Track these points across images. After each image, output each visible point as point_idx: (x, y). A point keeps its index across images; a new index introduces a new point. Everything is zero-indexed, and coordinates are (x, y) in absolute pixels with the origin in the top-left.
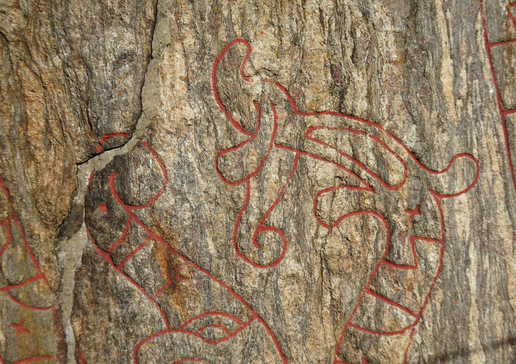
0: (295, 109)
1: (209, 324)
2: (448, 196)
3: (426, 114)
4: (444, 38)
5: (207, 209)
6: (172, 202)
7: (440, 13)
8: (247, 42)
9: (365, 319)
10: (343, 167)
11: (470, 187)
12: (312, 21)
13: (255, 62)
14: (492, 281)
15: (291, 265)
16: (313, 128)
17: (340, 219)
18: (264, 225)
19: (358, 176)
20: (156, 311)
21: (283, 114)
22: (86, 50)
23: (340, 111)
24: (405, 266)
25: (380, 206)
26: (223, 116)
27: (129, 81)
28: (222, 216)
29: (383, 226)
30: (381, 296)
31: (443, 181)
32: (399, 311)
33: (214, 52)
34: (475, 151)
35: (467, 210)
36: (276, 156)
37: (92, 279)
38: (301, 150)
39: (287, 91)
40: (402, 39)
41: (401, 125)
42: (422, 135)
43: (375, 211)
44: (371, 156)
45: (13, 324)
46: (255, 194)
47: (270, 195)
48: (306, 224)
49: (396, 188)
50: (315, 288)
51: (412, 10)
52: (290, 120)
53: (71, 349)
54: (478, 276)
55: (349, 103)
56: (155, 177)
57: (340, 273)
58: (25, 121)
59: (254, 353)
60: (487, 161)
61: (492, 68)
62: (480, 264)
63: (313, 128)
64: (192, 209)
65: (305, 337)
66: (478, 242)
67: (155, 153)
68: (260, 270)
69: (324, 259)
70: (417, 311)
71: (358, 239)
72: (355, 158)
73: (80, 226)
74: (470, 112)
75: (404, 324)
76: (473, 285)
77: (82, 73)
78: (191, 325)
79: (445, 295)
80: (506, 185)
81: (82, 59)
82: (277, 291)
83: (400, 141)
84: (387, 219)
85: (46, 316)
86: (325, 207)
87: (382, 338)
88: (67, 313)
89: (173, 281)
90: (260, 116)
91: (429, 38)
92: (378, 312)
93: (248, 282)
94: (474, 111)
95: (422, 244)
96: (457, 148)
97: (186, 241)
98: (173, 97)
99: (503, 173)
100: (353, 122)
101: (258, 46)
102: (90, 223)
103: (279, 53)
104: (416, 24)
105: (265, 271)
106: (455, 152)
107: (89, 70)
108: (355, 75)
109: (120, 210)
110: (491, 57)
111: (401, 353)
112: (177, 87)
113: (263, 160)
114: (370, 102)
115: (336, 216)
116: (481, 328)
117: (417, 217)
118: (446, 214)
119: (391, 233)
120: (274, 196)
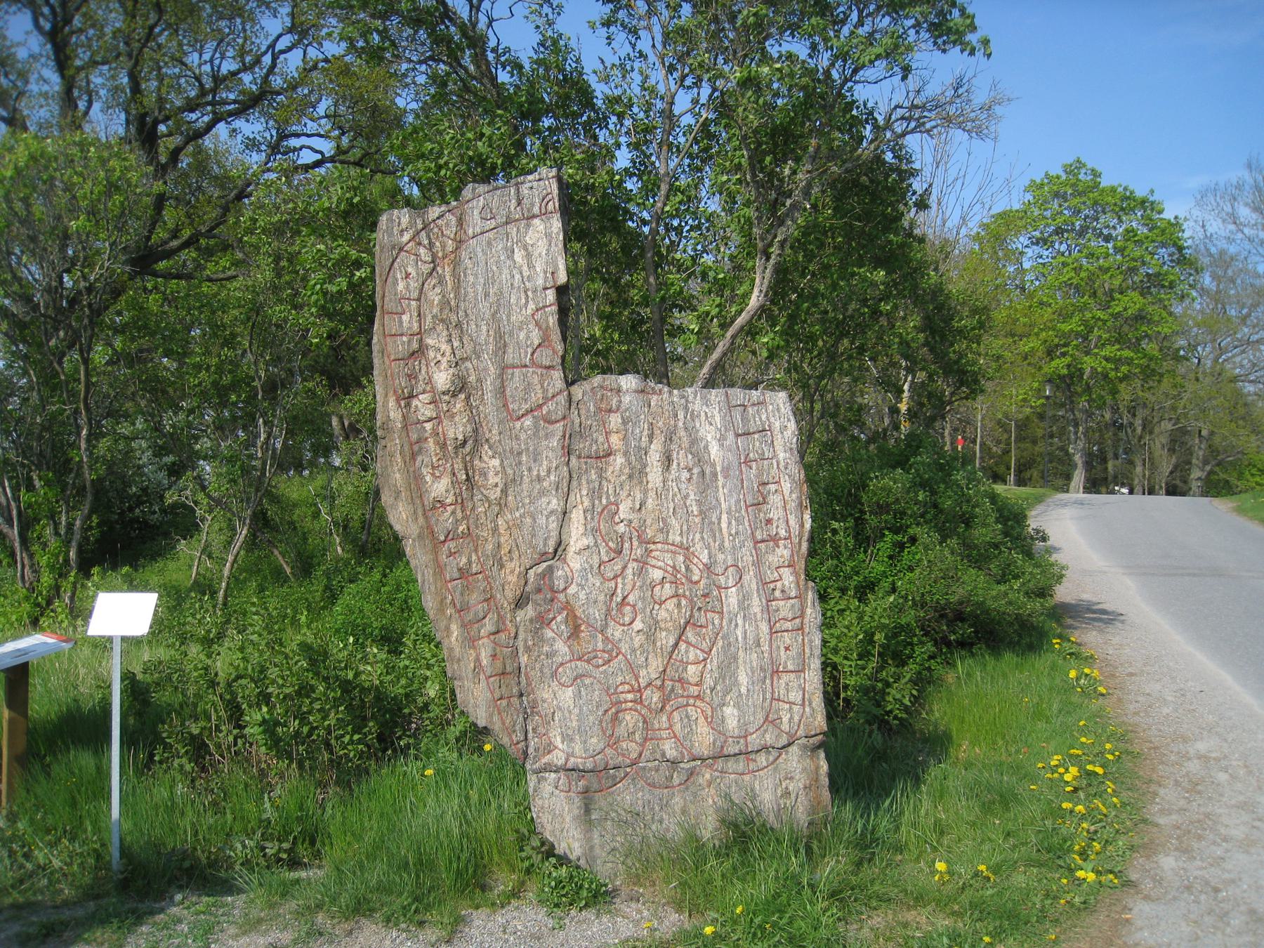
0: (643, 541)
8: (617, 505)
12: (652, 494)
14: (751, 636)
21: (635, 543)
27: (555, 525)
30: (689, 643)
31: (722, 580)
43: (684, 596)
46: (620, 586)
47: (629, 587)
49: (697, 583)
72: (674, 567)
84: (691, 601)
88: (521, 651)
92: (687, 652)
113: (625, 567)
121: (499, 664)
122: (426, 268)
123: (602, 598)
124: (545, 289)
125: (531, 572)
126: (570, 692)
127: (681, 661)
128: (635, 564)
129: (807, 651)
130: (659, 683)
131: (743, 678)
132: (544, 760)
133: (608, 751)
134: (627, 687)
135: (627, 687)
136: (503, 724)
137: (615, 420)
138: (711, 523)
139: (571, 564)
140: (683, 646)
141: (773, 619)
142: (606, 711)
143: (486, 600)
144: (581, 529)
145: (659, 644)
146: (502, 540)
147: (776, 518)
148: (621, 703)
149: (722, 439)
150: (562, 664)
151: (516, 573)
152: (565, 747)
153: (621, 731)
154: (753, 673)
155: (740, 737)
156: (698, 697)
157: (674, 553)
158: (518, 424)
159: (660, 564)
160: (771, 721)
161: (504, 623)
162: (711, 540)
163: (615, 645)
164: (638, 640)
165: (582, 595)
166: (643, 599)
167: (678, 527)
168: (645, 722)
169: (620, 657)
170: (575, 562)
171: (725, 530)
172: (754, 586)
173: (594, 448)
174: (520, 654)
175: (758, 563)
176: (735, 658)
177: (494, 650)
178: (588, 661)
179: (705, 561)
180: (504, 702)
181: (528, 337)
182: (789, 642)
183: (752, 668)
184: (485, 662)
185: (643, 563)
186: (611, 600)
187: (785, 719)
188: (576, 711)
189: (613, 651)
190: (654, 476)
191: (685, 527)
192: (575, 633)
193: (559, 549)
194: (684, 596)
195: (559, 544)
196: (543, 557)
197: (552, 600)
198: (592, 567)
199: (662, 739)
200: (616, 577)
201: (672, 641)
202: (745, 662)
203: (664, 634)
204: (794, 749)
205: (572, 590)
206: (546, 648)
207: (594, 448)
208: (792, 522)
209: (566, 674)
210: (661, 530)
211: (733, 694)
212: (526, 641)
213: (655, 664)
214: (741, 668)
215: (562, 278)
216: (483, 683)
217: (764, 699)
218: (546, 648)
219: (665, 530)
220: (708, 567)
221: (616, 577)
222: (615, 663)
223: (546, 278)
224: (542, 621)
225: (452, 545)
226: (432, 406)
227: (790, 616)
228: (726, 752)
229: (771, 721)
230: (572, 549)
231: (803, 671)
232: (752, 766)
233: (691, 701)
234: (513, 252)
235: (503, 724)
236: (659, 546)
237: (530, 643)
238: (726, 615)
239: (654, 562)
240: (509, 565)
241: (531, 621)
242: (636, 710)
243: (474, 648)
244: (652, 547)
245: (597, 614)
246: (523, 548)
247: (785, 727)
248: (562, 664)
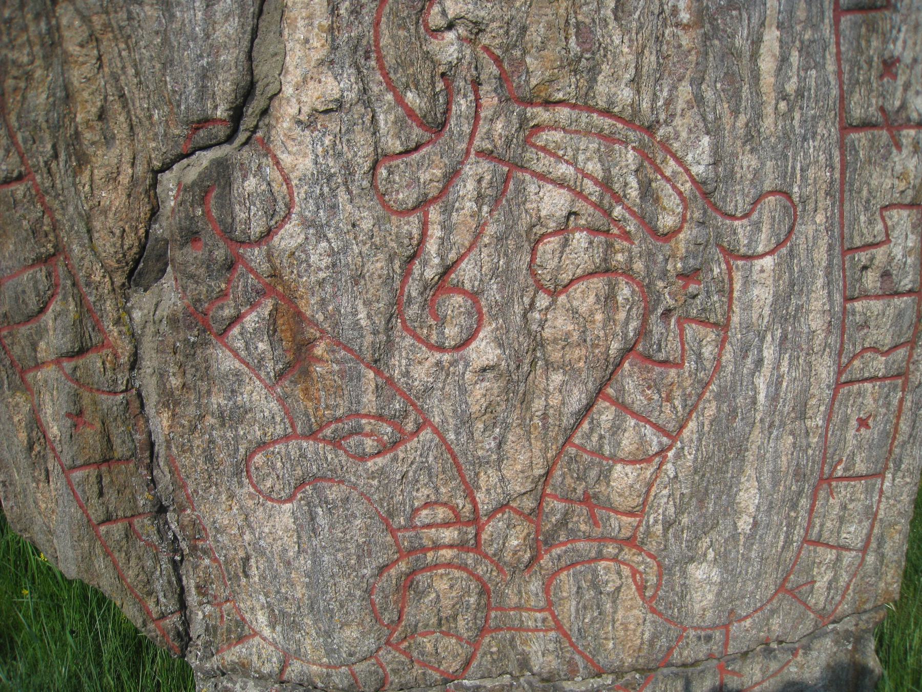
1: (357, 431)
3: (727, 120)
9: (595, 438)
10: (586, 199)
11: (779, 245)
16: (538, 128)
17: (571, 282)
19: (608, 213)
20: (274, 405)
21: (490, 101)
24: (665, 363)
26: (389, 97)
30: (624, 407)
32: (648, 431)
35: (770, 282)
36: (476, 173)
39: (498, 61)
41: (684, 135)
43: (628, 273)
44: (633, 182)
46: (436, 232)
47: (462, 238)
49: (669, 236)
55: (602, 88)
58: (67, 96)
62: (777, 366)
63: (538, 128)
64: (332, 253)
66: (778, 333)
68: (438, 355)
72: (606, 184)
73: (164, 271)
74: (796, 123)
75: (655, 448)
78: (328, 432)
79: (719, 409)
80: (830, 247)
82: (463, 390)
87: (619, 467)
94: (803, 122)
97: (323, 302)
105: (446, 357)
110: (837, 33)
113: (452, 176)
115: (565, 277)
118: (737, 286)
121: (91, 435)
123: (377, 265)
125: (168, 180)
126: (285, 516)
127: (598, 452)
128: (485, 167)
129: (904, 427)
130: (528, 504)
131: (749, 497)
132: (232, 655)
133: (387, 656)
134: (441, 513)
135: (441, 513)
136: (121, 577)
138: (731, 53)
139: (286, 159)
140: (606, 414)
141: (848, 347)
142: (382, 569)
143: (41, 260)
144: (319, 47)
145: (538, 404)
146: (76, 76)
147: (908, 57)
148: (424, 549)
150: (262, 445)
151: (124, 179)
152: (279, 639)
153: (421, 612)
154: (775, 483)
155: (714, 627)
156: (630, 541)
157: (608, 138)
159: (564, 169)
160: (790, 590)
161: (98, 327)
162: (724, 108)
163: (414, 401)
164: (479, 394)
165: (318, 256)
166: (505, 276)
167: (627, 54)
168: (484, 591)
169: (426, 435)
170: (298, 154)
171: (768, 80)
172: (821, 255)
174: (150, 410)
175: (841, 191)
176: (741, 450)
177: (76, 398)
178: (336, 442)
179: (698, 170)
180: (117, 529)
183: (775, 472)
184: (54, 430)
185: (510, 164)
186: (407, 273)
187: (821, 583)
188: (305, 563)
189: (406, 412)
191: (650, 59)
192: (297, 362)
193: (247, 110)
194: (628, 273)
195: (247, 92)
196: (198, 132)
197: (230, 266)
198: (348, 169)
199: (521, 629)
200: (423, 204)
201: (577, 399)
202: (761, 458)
203: (557, 378)
205: (290, 237)
206: (218, 400)
209: (274, 467)
210: (572, 65)
211: (719, 536)
212: (162, 375)
213: (523, 458)
214: (750, 471)
216: (57, 483)
217: (788, 542)
218: (218, 400)
219: (586, 63)
220: (705, 191)
221: (423, 204)
222: (410, 450)
224: (201, 325)
227: (888, 341)
229: (790, 590)
230: (288, 111)
231: (881, 475)
233: (611, 549)
235: (121, 577)
236: (564, 113)
237: (175, 382)
238: (736, 335)
239: (544, 163)
240: (104, 159)
241: (173, 321)
242: (463, 567)
243: (26, 388)
244: (542, 115)
245: (361, 314)
246: (140, 104)
247: (818, 599)
248: (262, 445)
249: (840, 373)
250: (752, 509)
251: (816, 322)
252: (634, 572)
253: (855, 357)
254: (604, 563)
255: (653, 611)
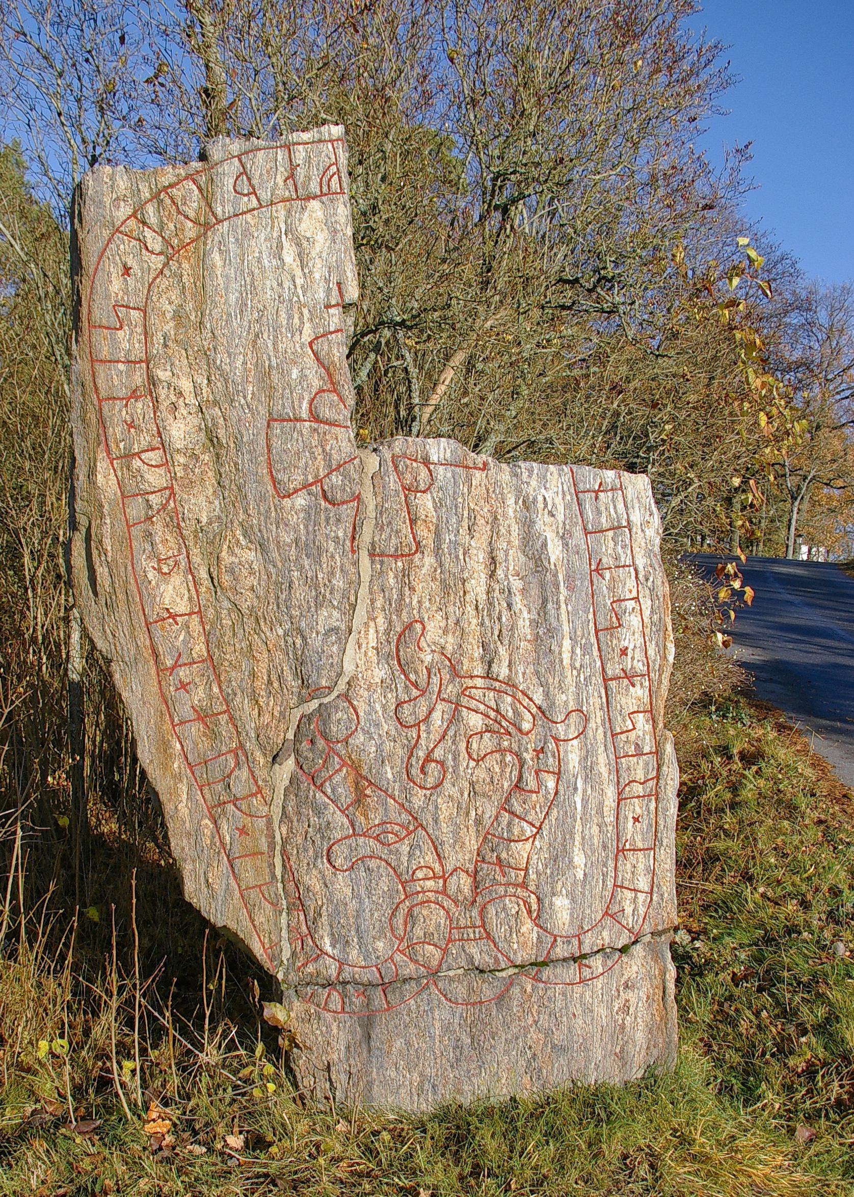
0: (455, 672)
2: (564, 740)
3: (551, 680)
4: (565, 624)
5: (388, 746)
6: (362, 740)
7: (563, 606)
9: (500, 829)
10: (489, 717)
12: (470, 609)
13: (428, 638)
14: (593, 804)
15: (449, 788)
17: (485, 756)
18: (428, 759)
19: (500, 724)
20: (345, 820)
21: (447, 677)
22: (303, 624)
23: (488, 676)
24: (531, 792)
25: (515, 747)
27: (335, 649)
28: (400, 752)
29: (516, 761)
30: (512, 813)
32: (525, 824)
33: (399, 629)
34: (584, 708)
35: (577, 751)
36: (440, 707)
37: (297, 796)
38: (458, 705)
39: (450, 661)
40: (535, 624)
42: (547, 694)
44: (509, 709)
45: (237, 829)
46: (423, 735)
48: (461, 758)
50: (464, 806)
51: (543, 603)
52: (451, 681)
53: (278, 848)
54: (583, 800)
56: (350, 720)
57: (484, 795)
58: (253, 675)
59: (418, 853)
60: (593, 716)
61: (599, 648)
62: (585, 791)
65: (455, 842)
67: (350, 702)
68: (424, 791)
69: (472, 784)
70: (538, 825)
71: (497, 770)
72: (497, 711)
73: (290, 755)
74: (582, 679)
75: (528, 834)
76: (579, 806)
77: (299, 641)
79: (558, 812)
81: (300, 632)
82: (436, 807)
83: (531, 699)
85: (261, 823)
86: (475, 746)
87: (512, 844)
89: (360, 799)
90: (429, 677)
91: (555, 624)
92: (509, 824)
93: (415, 800)
95: (544, 775)
96: (572, 706)
98: (362, 659)
99: (603, 724)
100: (497, 684)
101: (430, 626)
102: (297, 752)
103: (445, 631)
104: (545, 614)
105: (428, 792)
106: (570, 709)
107: (304, 638)
108: (500, 650)
109: (321, 743)
111: (526, 856)
112: (370, 654)
114: (510, 670)
115: (482, 754)
116: (583, 838)
117: (541, 756)
119: (522, 767)
120: (438, 738)
122: (157, 262)
124: (328, 306)
131: (579, 859)
137: (425, 503)
141: (621, 780)
147: (631, 647)
149: (565, 537)
158: (287, 502)
171: (567, 661)
173: (394, 541)
181: (303, 377)
182: (638, 811)
187: (629, 910)
190: (478, 586)
204: (638, 950)
207: (394, 541)
208: (651, 652)
215: (353, 293)
223: (328, 291)
225: (183, 673)
226: (162, 471)
228: (553, 957)
232: (587, 973)
233: (511, 890)
234: (280, 247)
244: (470, 683)
249: (619, 794)
250: (583, 866)
251: (604, 770)
252: (525, 902)
253: (626, 786)
254: (508, 898)
255: (537, 925)
